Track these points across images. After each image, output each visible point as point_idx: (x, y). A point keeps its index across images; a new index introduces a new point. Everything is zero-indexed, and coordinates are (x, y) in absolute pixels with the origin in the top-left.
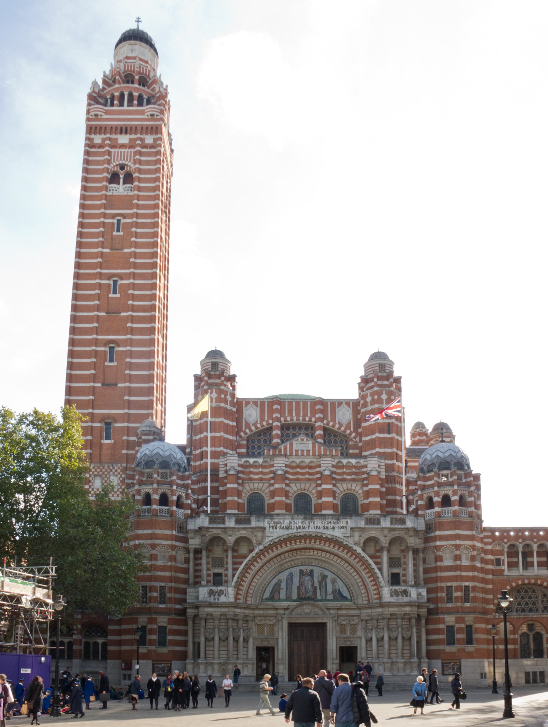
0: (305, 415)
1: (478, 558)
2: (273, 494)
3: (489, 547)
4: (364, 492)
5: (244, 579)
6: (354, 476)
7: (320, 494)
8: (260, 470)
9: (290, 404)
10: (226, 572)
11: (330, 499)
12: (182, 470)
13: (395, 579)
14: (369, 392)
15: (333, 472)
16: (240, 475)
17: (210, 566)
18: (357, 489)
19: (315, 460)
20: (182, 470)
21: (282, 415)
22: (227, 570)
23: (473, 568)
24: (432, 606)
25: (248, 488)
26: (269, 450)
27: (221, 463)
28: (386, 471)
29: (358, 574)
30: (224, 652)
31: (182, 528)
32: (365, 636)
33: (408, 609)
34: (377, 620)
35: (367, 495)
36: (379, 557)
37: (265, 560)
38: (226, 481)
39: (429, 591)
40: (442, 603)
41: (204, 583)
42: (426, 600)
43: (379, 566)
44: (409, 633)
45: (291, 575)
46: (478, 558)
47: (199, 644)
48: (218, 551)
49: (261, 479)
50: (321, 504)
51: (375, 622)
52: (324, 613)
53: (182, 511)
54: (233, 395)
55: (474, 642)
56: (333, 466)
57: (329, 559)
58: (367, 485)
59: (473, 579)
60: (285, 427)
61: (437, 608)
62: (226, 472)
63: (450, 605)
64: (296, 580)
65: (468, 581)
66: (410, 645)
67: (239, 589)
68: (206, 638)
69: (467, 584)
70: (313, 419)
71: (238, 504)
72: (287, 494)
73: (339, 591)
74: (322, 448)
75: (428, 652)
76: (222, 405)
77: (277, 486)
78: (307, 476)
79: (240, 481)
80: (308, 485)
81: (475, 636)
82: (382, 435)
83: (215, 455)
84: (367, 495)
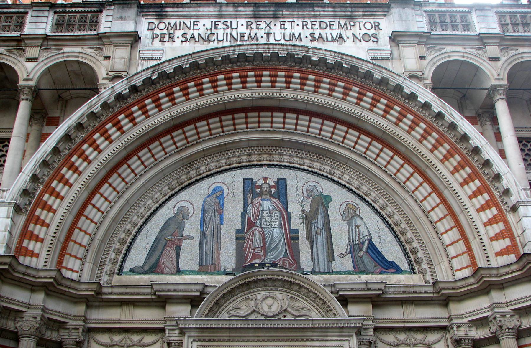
29: (427, 179)
73: (370, 241)
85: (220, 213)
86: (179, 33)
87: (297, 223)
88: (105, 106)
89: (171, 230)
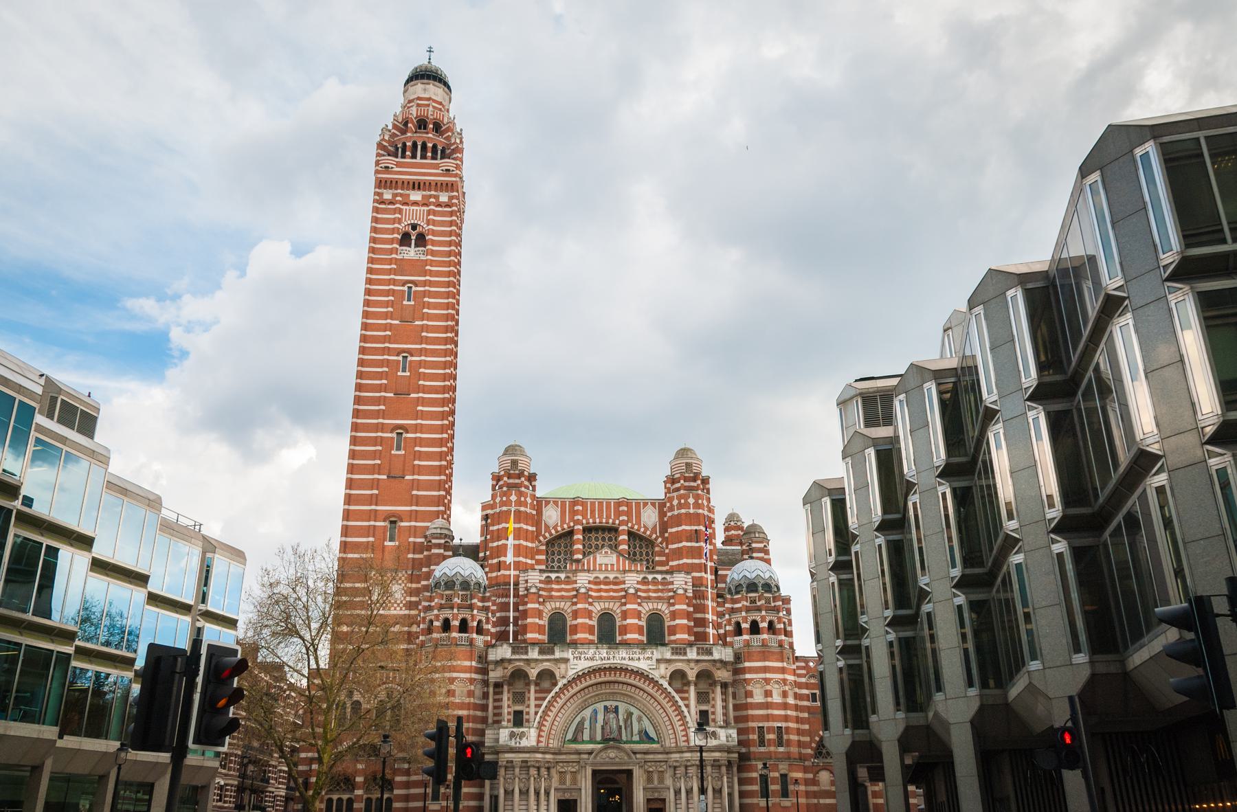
0: (608, 517)
1: (791, 694)
2: (575, 614)
3: (803, 680)
4: (670, 612)
5: (547, 718)
6: (660, 594)
7: (625, 615)
8: (563, 586)
9: (593, 504)
10: (527, 709)
11: (636, 621)
12: (482, 590)
13: (704, 720)
14: (675, 494)
15: (637, 590)
16: (541, 593)
17: (510, 703)
18: (663, 607)
19: (619, 576)
20: (482, 590)
21: (585, 517)
22: (528, 706)
23: (785, 706)
24: (744, 750)
25: (549, 608)
26: (572, 564)
27: (521, 579)
28: (693, 586)
30: (524, 807)
31: (482, 658)
32: (673, 785)
33: (717, 755)
34: (686, 767)
35: (674, 615)
36: (687, 692)
37: (568, 695)
38: (526, 600)
39: (740, 732)
40: (754, 746)
41: (504, 723)
42: (736, 743)
43: (686, 702)
44: (719, 783)
45: (595, 712)
46: (791, 694)
47: (496, 797)
48: (519, 686)
49: (562, 597)
50: (625, 626)
51: (683, 769)
52: (630, 757)
53: (482, 637)
54: (533, 497)
55: (790, 795)
56: (638, 583)
57: (634, 693)
58: (673, 605)
59: (786, 718)
60: (587, 530)
61: (749, 753)
62: (527, 589)
63: (762, 749)
64: (600, 717)
65: (781, 721)
66: (721, 798)
67: (541, 730)
68: (505, 791)
69: (779, 725)
70: (617, 522)
71: (539, 625)
72: (589, 614)
74: (627, 562)
75: (741, 805)
76: (522, 509)
77: (580, 606)
78: (612, 594)
79: (541, 600)
80: (612, 604)
81: (791, 787)
82: (689, 544)
83: (517, 565)
84: (674, 615)
85: (596, 719)
86: (583, 656)
87: (622, 723)
88: (560, 689)
89: (580, 725)
